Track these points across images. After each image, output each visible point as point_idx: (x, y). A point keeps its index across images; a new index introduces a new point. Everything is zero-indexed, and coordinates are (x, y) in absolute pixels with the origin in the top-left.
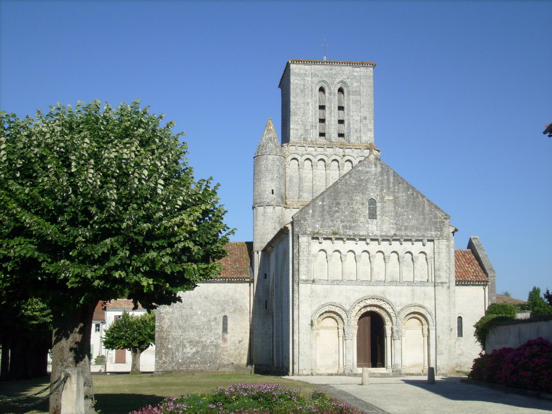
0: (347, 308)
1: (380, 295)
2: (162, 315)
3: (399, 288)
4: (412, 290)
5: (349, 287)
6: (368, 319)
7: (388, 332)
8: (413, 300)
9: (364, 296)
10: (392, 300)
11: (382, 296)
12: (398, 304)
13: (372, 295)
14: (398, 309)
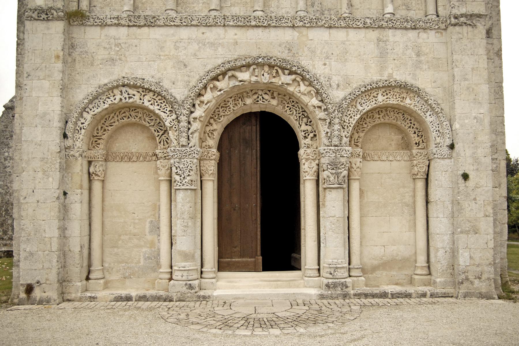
0: (179, 92)
1: (278, 53)
2: (8, 170)
3: (340, 35)
4: (379, 40)
5: (185, 33)
6: (253, 132)
7: (307, 169)
8: (382, 68)
9: (230, 56)
10: (317, 68)
11: (285, 55)
12: (335, 80)
13: (255, 53)
14: (337, 95)
